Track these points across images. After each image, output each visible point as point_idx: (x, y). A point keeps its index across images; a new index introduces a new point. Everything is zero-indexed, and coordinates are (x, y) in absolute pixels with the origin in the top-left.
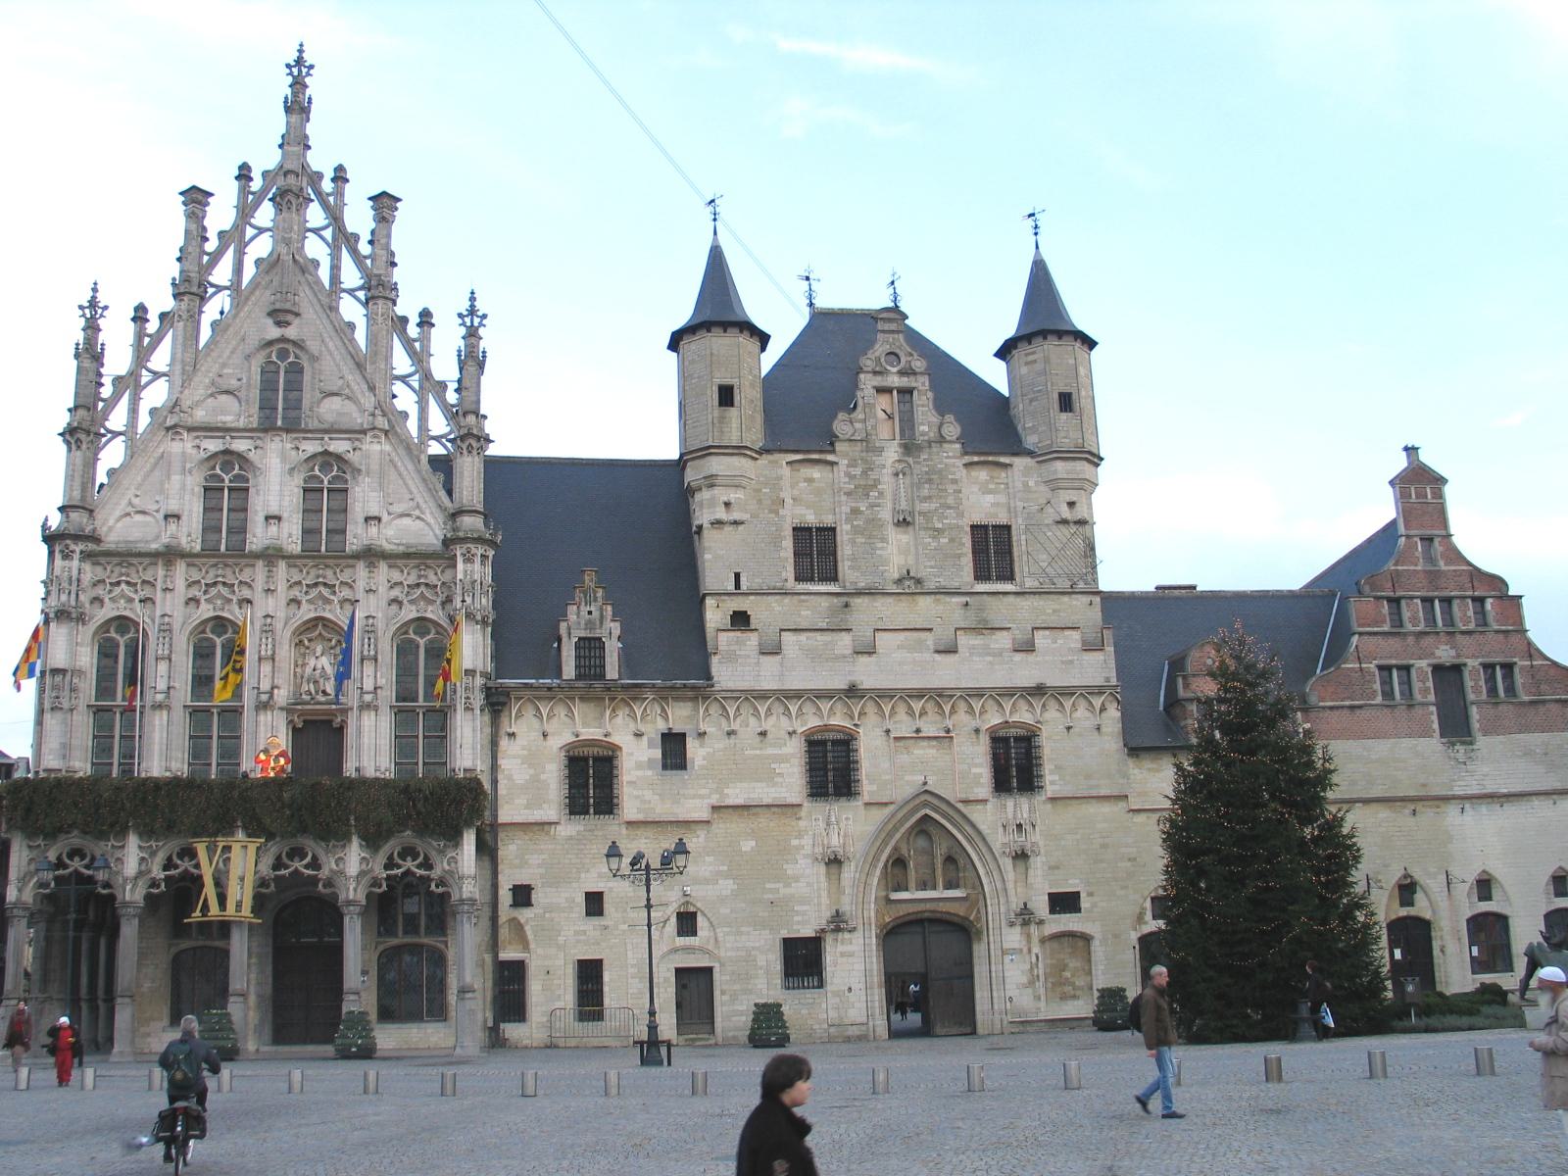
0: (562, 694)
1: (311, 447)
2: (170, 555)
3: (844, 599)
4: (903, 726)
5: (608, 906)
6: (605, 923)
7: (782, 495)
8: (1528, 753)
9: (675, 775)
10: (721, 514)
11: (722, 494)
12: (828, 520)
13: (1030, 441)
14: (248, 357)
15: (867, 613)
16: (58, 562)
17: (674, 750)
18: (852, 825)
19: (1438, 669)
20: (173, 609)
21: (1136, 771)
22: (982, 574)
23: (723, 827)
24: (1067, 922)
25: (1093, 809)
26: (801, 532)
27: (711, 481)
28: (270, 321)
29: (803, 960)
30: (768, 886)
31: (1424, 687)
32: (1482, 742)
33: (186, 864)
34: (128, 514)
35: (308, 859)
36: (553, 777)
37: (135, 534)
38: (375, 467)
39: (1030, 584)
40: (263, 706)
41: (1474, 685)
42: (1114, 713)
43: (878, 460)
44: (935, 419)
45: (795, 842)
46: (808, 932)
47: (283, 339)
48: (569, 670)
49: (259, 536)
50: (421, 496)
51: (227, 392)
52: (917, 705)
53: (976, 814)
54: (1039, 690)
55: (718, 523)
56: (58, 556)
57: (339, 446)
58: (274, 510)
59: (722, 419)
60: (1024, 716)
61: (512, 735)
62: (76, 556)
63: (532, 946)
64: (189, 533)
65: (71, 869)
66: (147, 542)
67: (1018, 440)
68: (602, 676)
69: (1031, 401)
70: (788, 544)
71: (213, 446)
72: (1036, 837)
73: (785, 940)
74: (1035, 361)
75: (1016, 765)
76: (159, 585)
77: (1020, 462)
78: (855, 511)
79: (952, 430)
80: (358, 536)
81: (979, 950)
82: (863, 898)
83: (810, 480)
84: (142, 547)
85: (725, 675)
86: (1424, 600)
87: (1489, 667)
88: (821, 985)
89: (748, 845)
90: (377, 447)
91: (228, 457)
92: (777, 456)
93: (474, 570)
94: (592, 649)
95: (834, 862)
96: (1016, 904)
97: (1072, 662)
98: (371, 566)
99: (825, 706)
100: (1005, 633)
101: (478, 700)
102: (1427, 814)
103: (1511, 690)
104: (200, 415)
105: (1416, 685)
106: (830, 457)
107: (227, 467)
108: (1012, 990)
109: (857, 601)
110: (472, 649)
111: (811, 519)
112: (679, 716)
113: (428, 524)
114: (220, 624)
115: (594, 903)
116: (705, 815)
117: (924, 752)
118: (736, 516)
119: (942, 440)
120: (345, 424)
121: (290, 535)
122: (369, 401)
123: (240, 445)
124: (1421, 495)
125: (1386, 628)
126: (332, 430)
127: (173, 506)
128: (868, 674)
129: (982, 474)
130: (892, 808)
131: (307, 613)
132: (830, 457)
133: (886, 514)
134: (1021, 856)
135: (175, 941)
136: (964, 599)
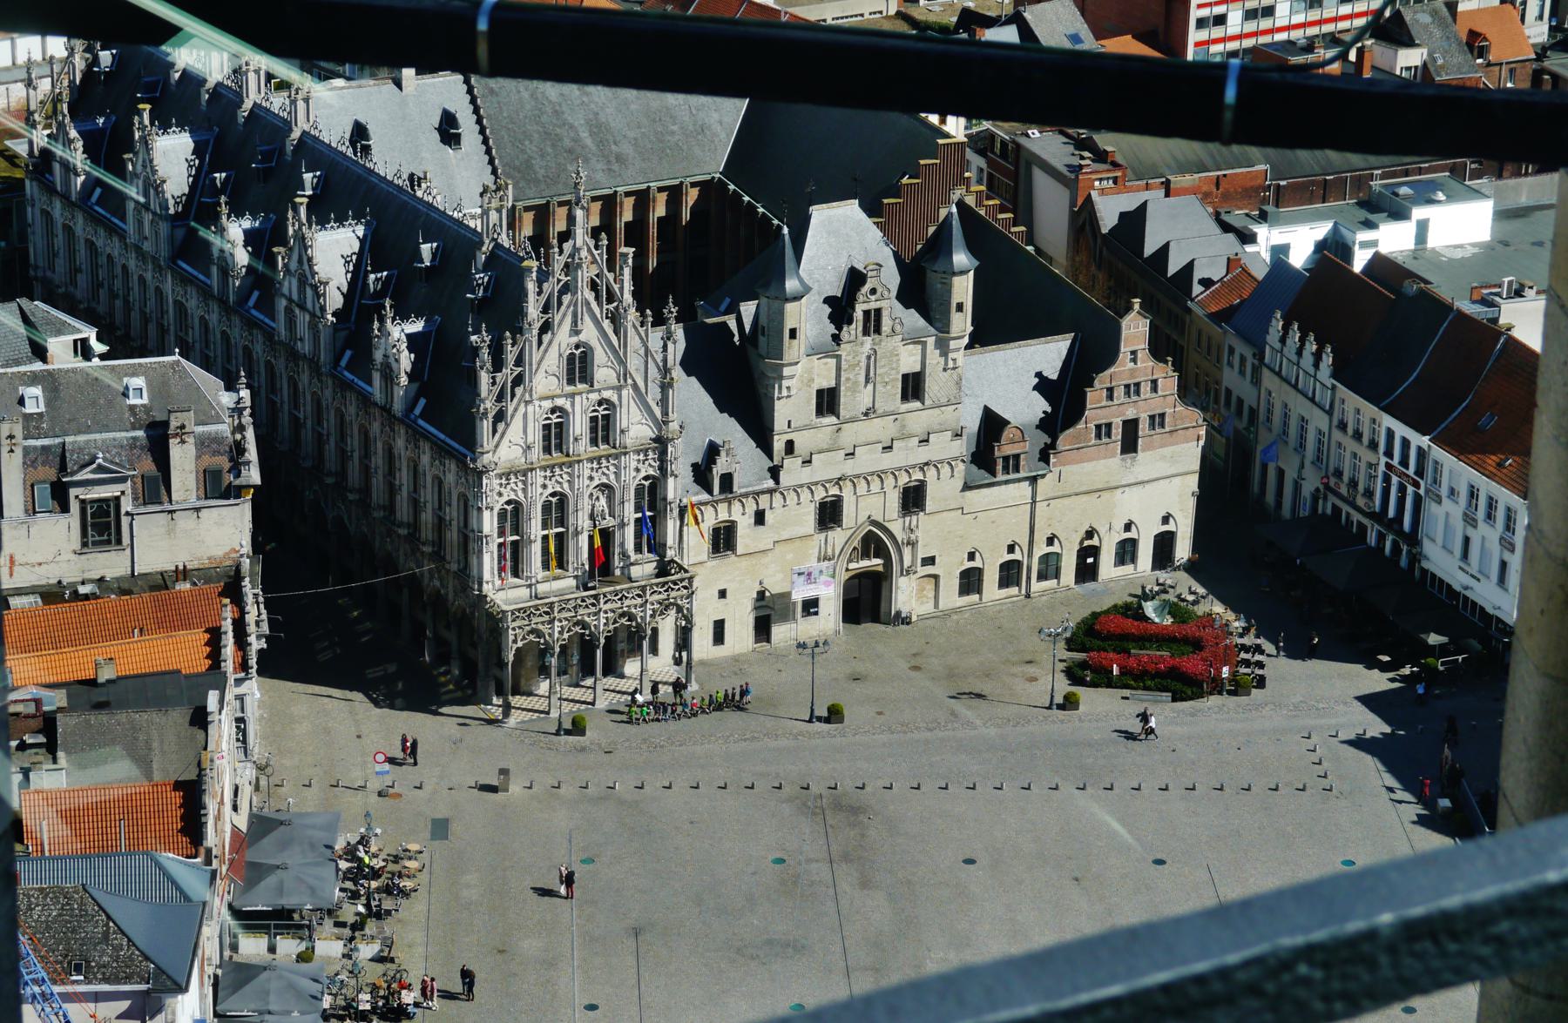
0: (714, 504)
1: (595, 397)
8: (1163, 458)
15: (850, 434)
17: (760, 518)
18: (837, 537)
19: (1125, 423)
20: (538, 493)
22: (905, 397)
23: (779, 548)
24: (930, 570)
26: (820, 393)
31: (1117, 433)
32: (1141, 455)
37: (512, 457)
41: (1144, 427)
48: (716, 490)
53: (891, 526)
57: (607, 394)
58: (578, 432)
64: (537, 454)
71: (547, 404)
75: (913, 499)
86: (1127, 386)
87: (1152, 418)
94: (727, 480)
101: (676, 512)
102: (1105, 495)
103: (1162, 425)
111: (828, 382)
115: (723, 594)
123: (560, 402)
125: (1104, 403)
128: (850, 468)
133: (862, 379)
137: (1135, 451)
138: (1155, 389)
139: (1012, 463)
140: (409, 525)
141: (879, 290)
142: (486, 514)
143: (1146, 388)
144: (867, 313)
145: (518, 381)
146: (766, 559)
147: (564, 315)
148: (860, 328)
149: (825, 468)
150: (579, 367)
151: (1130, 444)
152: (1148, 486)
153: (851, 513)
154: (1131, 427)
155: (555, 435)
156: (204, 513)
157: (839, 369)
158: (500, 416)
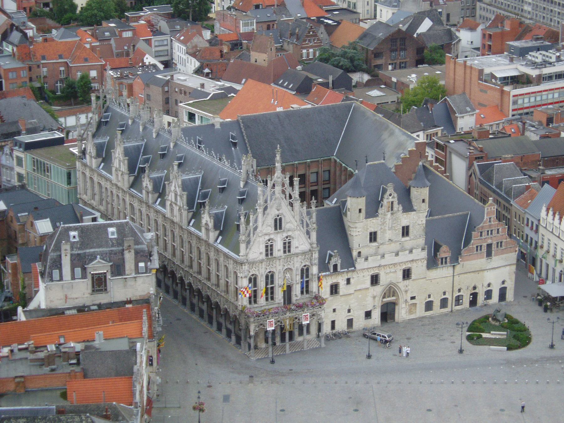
1: (285, 235)
2: (261, 262)
4: (388, 270)
5: (336, 310)
9: (349, 285)
10: (357, 234)
12: (376, 230)
13: (415, 208)
18: (378, 290)
23: (356, 293)
25: (420, 280)
29: (368, 314)
31: (484, 249)
32: (494, 258)
36: (328, 289)
41: (494, 247)
42: (426, 262)
43: (386, 217)
44: (397, 206)
46: (369, 310)
48: (332, 271)
49: (276, 253)
50: (304, 240)
51: (269, 226)
52: (391, 266)
53: (400, 285)
54: (412, 261)
57: (290, 233)
58: (279, 248)
59: (359, 216)
60: (408, 265)
64: (263, 256)
70: (369, 237)
71: (267, 238)
72: (409, 287)
73: (366, 312)
75: (407, 274)
76: (260, 267)
77: (413, 213)
78: (381, 228)
79: (401, 208)
80: (293, 250)
81: (397, 307)
82: (378, 303)
85: (358, 266)
88: (371, 318)
89: (360, 296)
93: (316, 255)
94: (335, 267)
95: (374, 297)
96: (405, 299)
98: (297, 256)
99: (375, 269)
102: (481, 273)
105: (483, 248)
108: (402, 315)
110: (315, 270)
112: (350, 275)
115: (334, 310)
117: (392, 274)
122: (296, 224)
123: (272, 237)
124: (491, 209)
126: (289, 231)
127: (261, 251)
128: (383, 262)
131: (286, 267)
133: (387, 228)
134: (406, 291)
137: (491, 256)
138: (498, 232)
139: (444, 261)
143: (495, 232)
145: (255, 229)
146: (352, 296)
149: (373, 262)
150: (278, 224)
151: (489, 254)
152: (497, 270)
153: (384, 280)
154: (489, 246)
155: (269, 250)
156: (138, 279)
158: (248, 243)
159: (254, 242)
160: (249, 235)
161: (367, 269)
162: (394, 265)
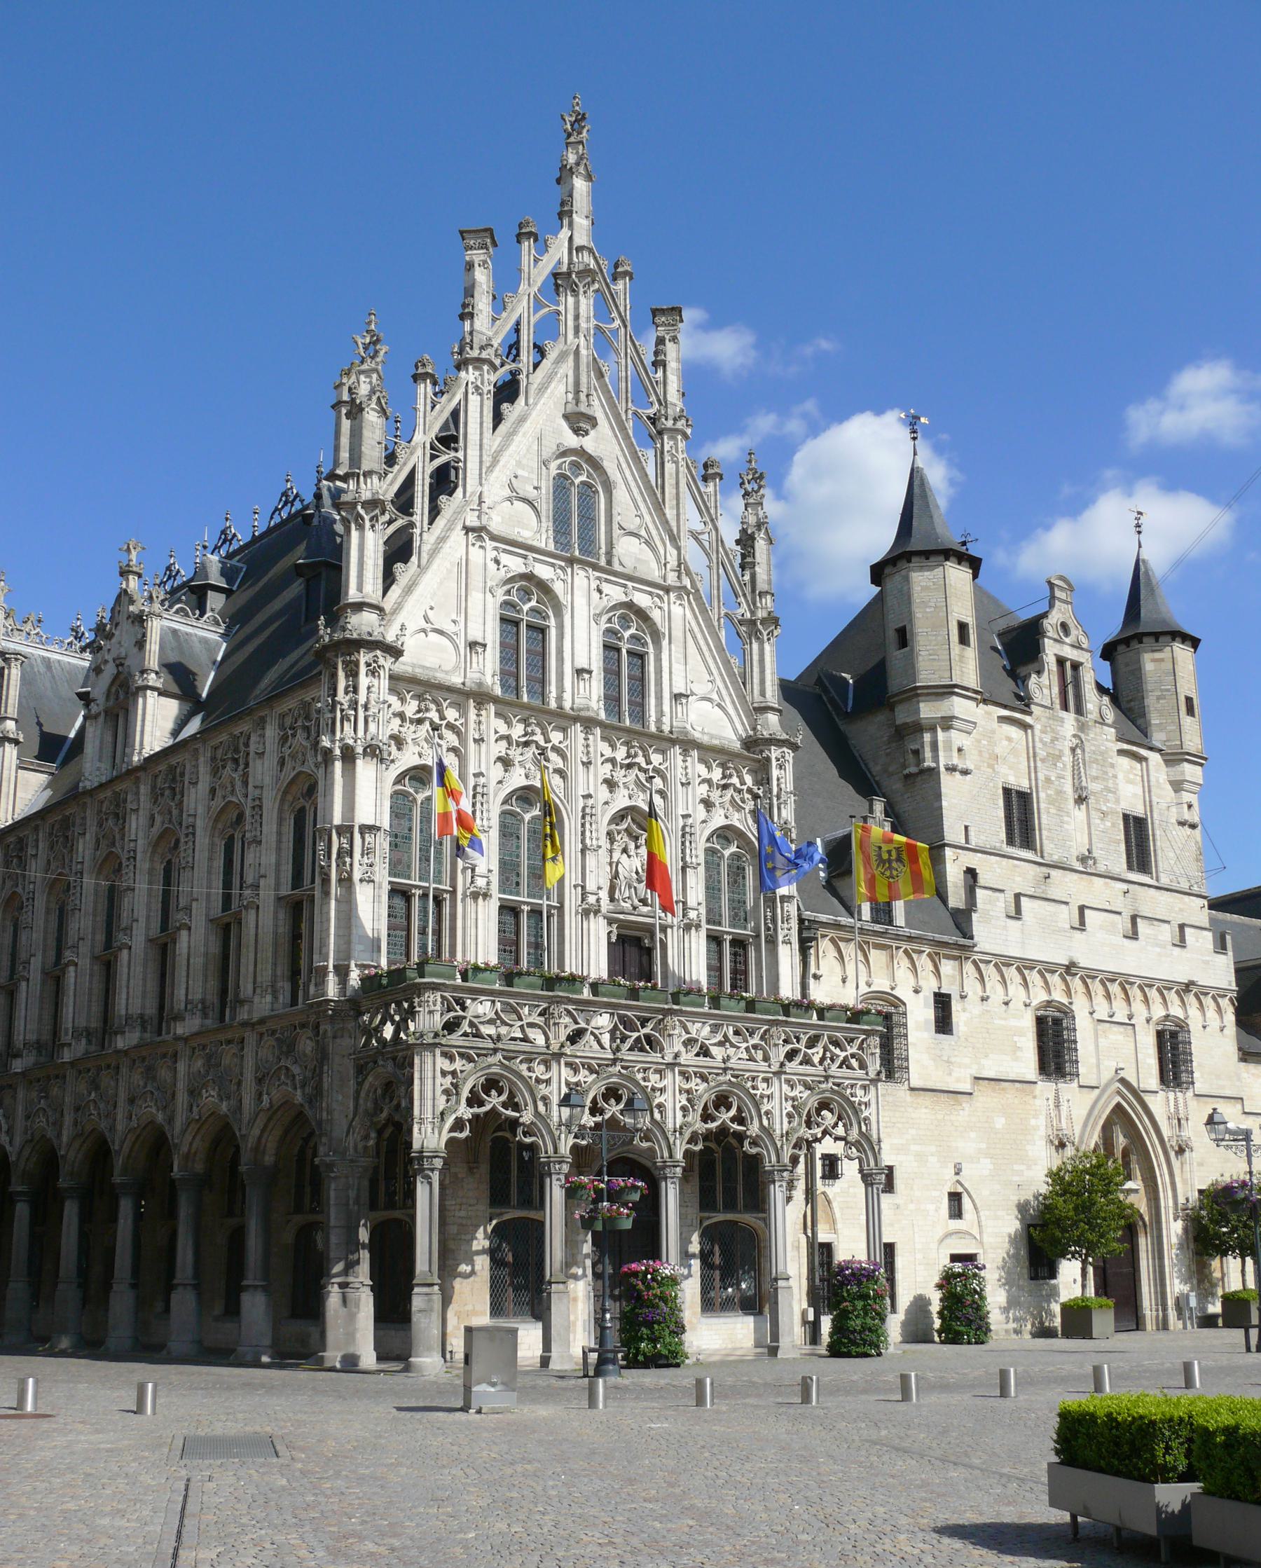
1: (615, 594)
2: (481, 697)
3: (1044, 870)
6: (897, 1201)
7: (998, 750)
10: (955, 761)
11: (957, 738)
14: (545, 463)
16: (364, 681)
21: (1245, 1075)
27: (947, 723)
28: (564, 425)
30: (1016, 1167)
33: (614, 1109)
34: (424, 631)
35: (733, 1112)
38: (677, 633)
39: (1165, 880)
40: (588, 912)
45: (1033, 1122)
47: (581, 452)
55: (951, 769)
56: (363, 669)
57: (642, 600)
58: (582, 663)
59: (962, 656)
61: (816, 977)
62: (384, 675)
63: (839, 1226)
65: (488, 1107)
66: (447, 672)
67: (1145, 732)
68: (890, 923)
69: (1159, 698)
70: (1001, 803)
71: (515, 565)
74: (1162, 660)
76: (472, 734)
83: (1009, 739)
84: (441, 677)
89: (1000, 1122)
90: (677, 610)
91: (530, 583)
92: (991, 708)
97: (1207, 962)
100: (1166, 925)
104: (496, 523)
106: (1028, 719)
107: (526, 594)
109: (1054, 873)
113: (727, 714)
114: (526, 795)
116: (966, 1087)
118: (969, 765)
119: (1102, 722)
120: (640, 574)
121: (591, 696)
123: (544, 572)
127: (475, 634)
129: (1125, 762)
130: (1097, 1091)
132: (1028, 719)
135: (498, 1211)
136: (1125, 886)
140: (143, 1021)
141: (1075, 632)
142: (365, 770)
144: (1061, 661)
145: (444, 481)
146: (964, 1113)
147: (550, 377)
148: (1056, 690)
149: (1041, 936)
157: (1032, 756)
159: (434, 552)
160: (404, 500)
161: (1024, 966)
162: (1125, 982)
